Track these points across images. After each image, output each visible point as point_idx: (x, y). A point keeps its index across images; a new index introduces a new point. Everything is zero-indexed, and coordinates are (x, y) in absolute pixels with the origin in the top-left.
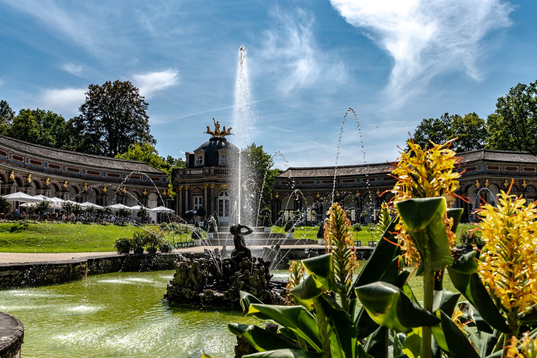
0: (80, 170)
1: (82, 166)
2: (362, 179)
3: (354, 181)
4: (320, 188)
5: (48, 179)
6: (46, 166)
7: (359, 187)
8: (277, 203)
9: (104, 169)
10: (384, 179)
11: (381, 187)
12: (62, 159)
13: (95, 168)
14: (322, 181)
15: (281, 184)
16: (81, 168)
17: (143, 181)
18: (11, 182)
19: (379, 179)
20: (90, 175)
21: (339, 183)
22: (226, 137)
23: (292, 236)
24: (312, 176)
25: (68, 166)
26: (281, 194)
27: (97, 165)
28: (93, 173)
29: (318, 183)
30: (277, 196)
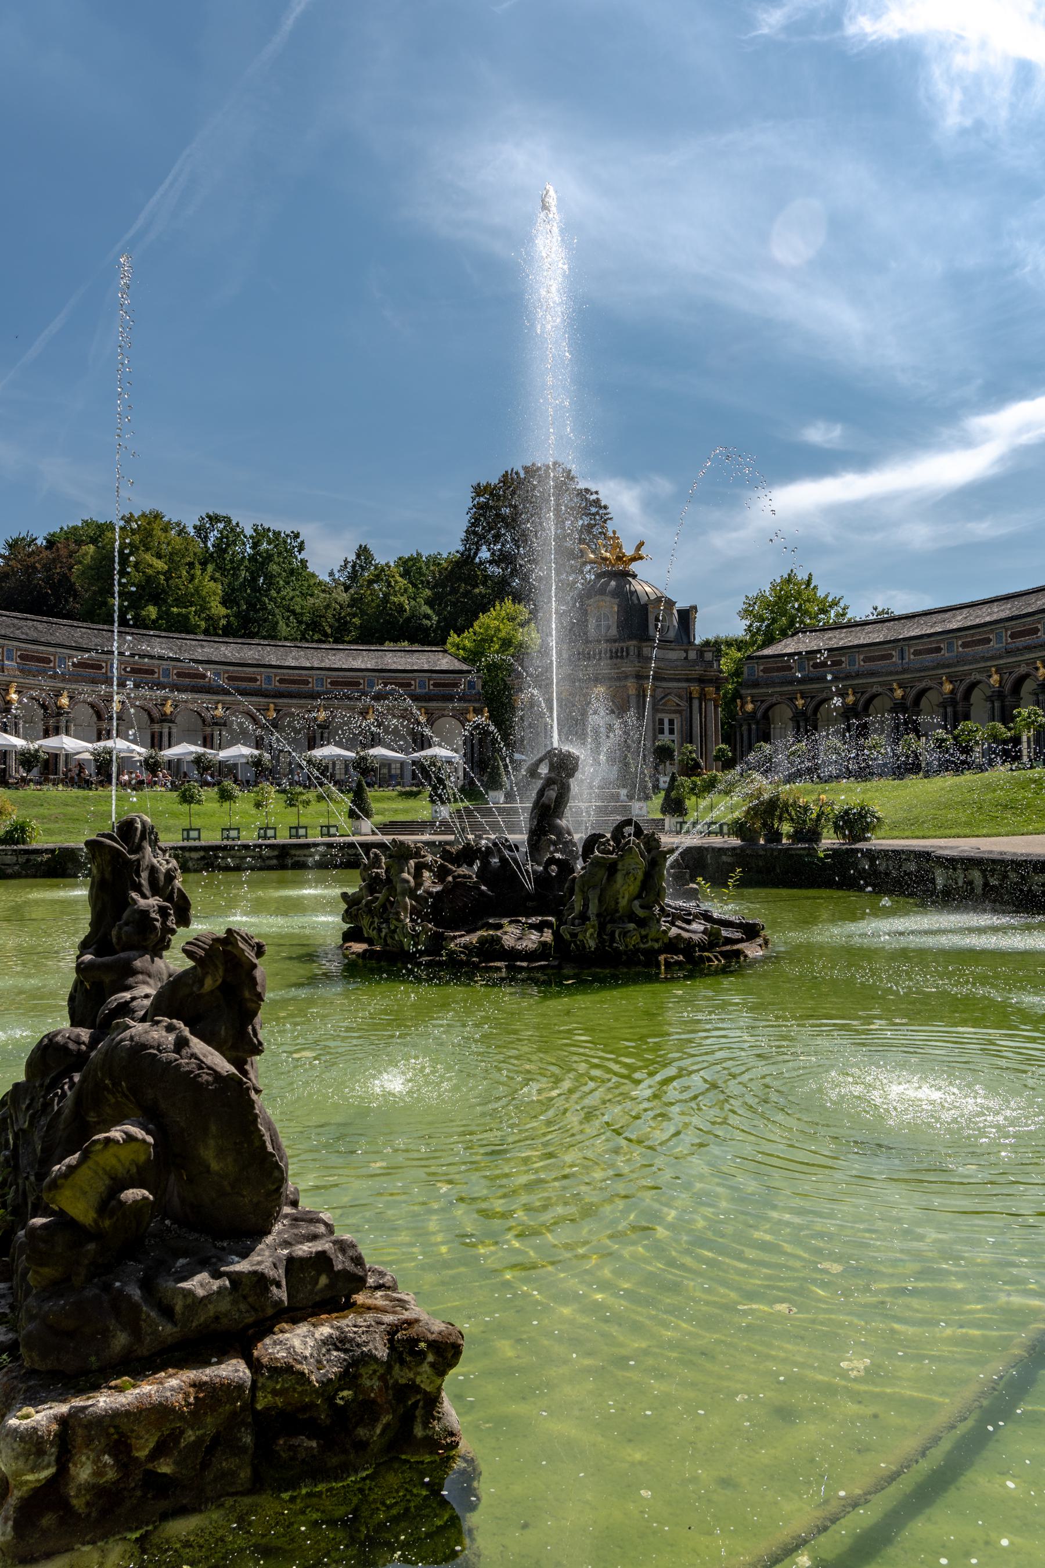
0: (259, 677)
1: (262, 670)
2: (960, 642)
3: (938, 650)
4: (858, 675)
5: (170, 702)
6: (168, 676)
7: (948, 666)
8: (749, 725)
9: (318, 672)
10: (1012, 636)
11: (1002, 662)
12: (214, 658)
13: (297, 672)
14: (862, 657)
15: (761, 674)
16: (261, 674)
17: (418, 691)
18: (59, 711)
19: (999, 638)
20: (284, 687)
21: (903, 659)
22: (634, 567)
23: (644, 812)
24: (841, 644)
25: (227, 672)
26: (762, 701)
27: (308, 665)
28: (293, 682)
29: (852, 662)
30: (750, 707)
